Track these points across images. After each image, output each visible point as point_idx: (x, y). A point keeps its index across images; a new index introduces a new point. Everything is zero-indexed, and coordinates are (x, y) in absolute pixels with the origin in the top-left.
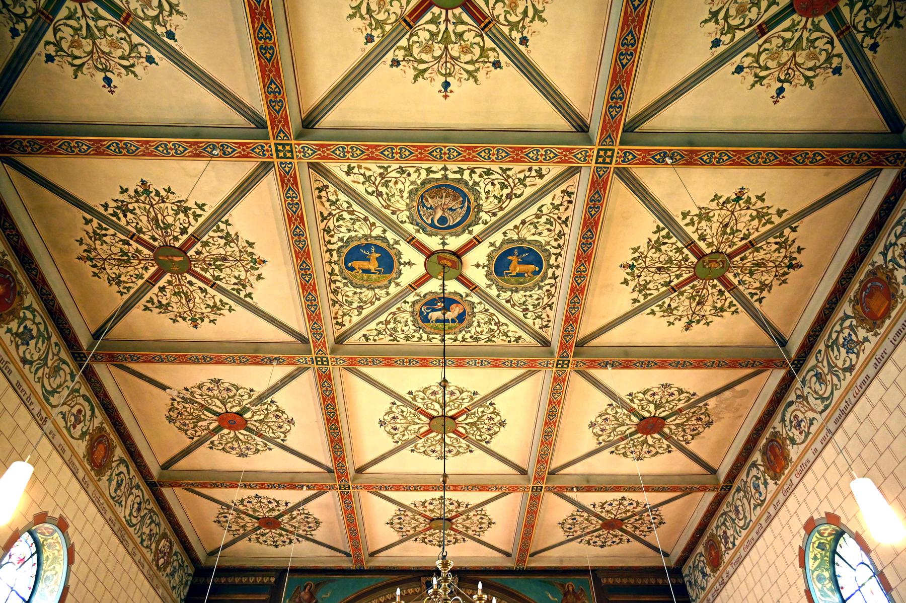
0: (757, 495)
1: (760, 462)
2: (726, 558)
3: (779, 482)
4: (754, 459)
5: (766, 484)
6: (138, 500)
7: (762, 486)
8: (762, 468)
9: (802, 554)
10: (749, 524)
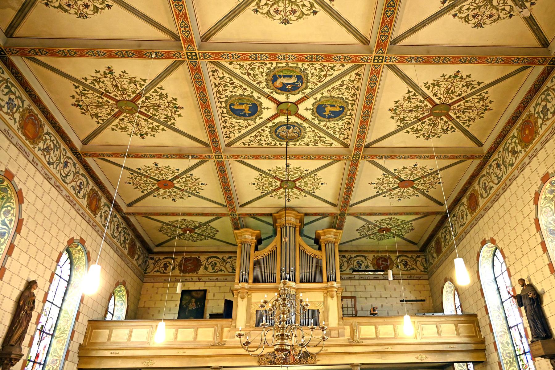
1: (466, 203)
5: (467, 215)
6: (116, 224)
7: (465, 216)
8: (466, 207)
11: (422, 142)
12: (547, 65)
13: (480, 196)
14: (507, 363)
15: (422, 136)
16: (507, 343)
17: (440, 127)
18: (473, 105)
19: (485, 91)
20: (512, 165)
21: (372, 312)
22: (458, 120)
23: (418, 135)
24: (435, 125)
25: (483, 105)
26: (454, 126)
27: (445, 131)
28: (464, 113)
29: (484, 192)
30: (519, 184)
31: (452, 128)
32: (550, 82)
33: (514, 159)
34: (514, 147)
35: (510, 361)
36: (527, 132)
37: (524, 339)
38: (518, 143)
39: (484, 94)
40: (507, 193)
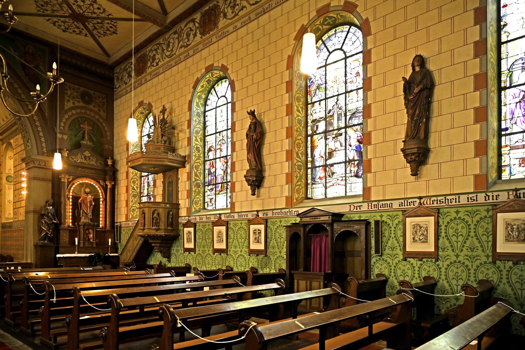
0: (186, 40)
2: (149, 70)
3: (203, 37)
4: (195, 17)
5: (195, 35)
8: (197, 25)
9: (198, 81)
10: (173, 55)
13: (222, 15)
29: (230, 11)
30: (261, 24)
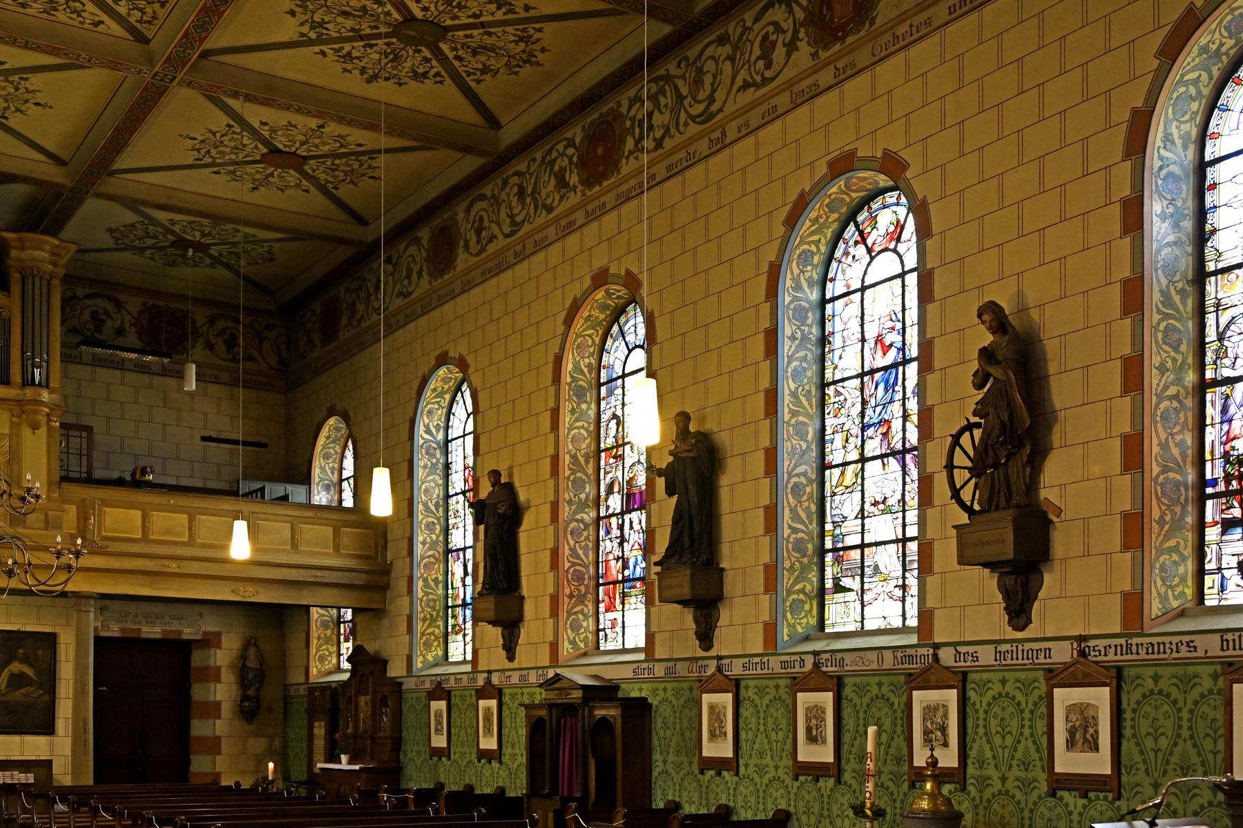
11: (354, 84)
12: (680, 27)
14: (424, 620)
15: (357, 72)
16: (436, 581)
17: (409, 64)
18: (502, 44)
19: (537, 26)
20: (550, 210)
21: (138, 476)
22: (457, 64)
23: (349, 67)
24: (396, 58)
25: (524, 51)
26: (443, 73)
27: (418, 77)
28: (475, 53)
31: (438, 74)
32: (674, 63)
33: (557, 197)
34: (565, 170)
35: (431, 615)
36: (600, 151)
37: (469, 580)
38: (576, 167)
39: (532, 31)
40: (521, 270)
